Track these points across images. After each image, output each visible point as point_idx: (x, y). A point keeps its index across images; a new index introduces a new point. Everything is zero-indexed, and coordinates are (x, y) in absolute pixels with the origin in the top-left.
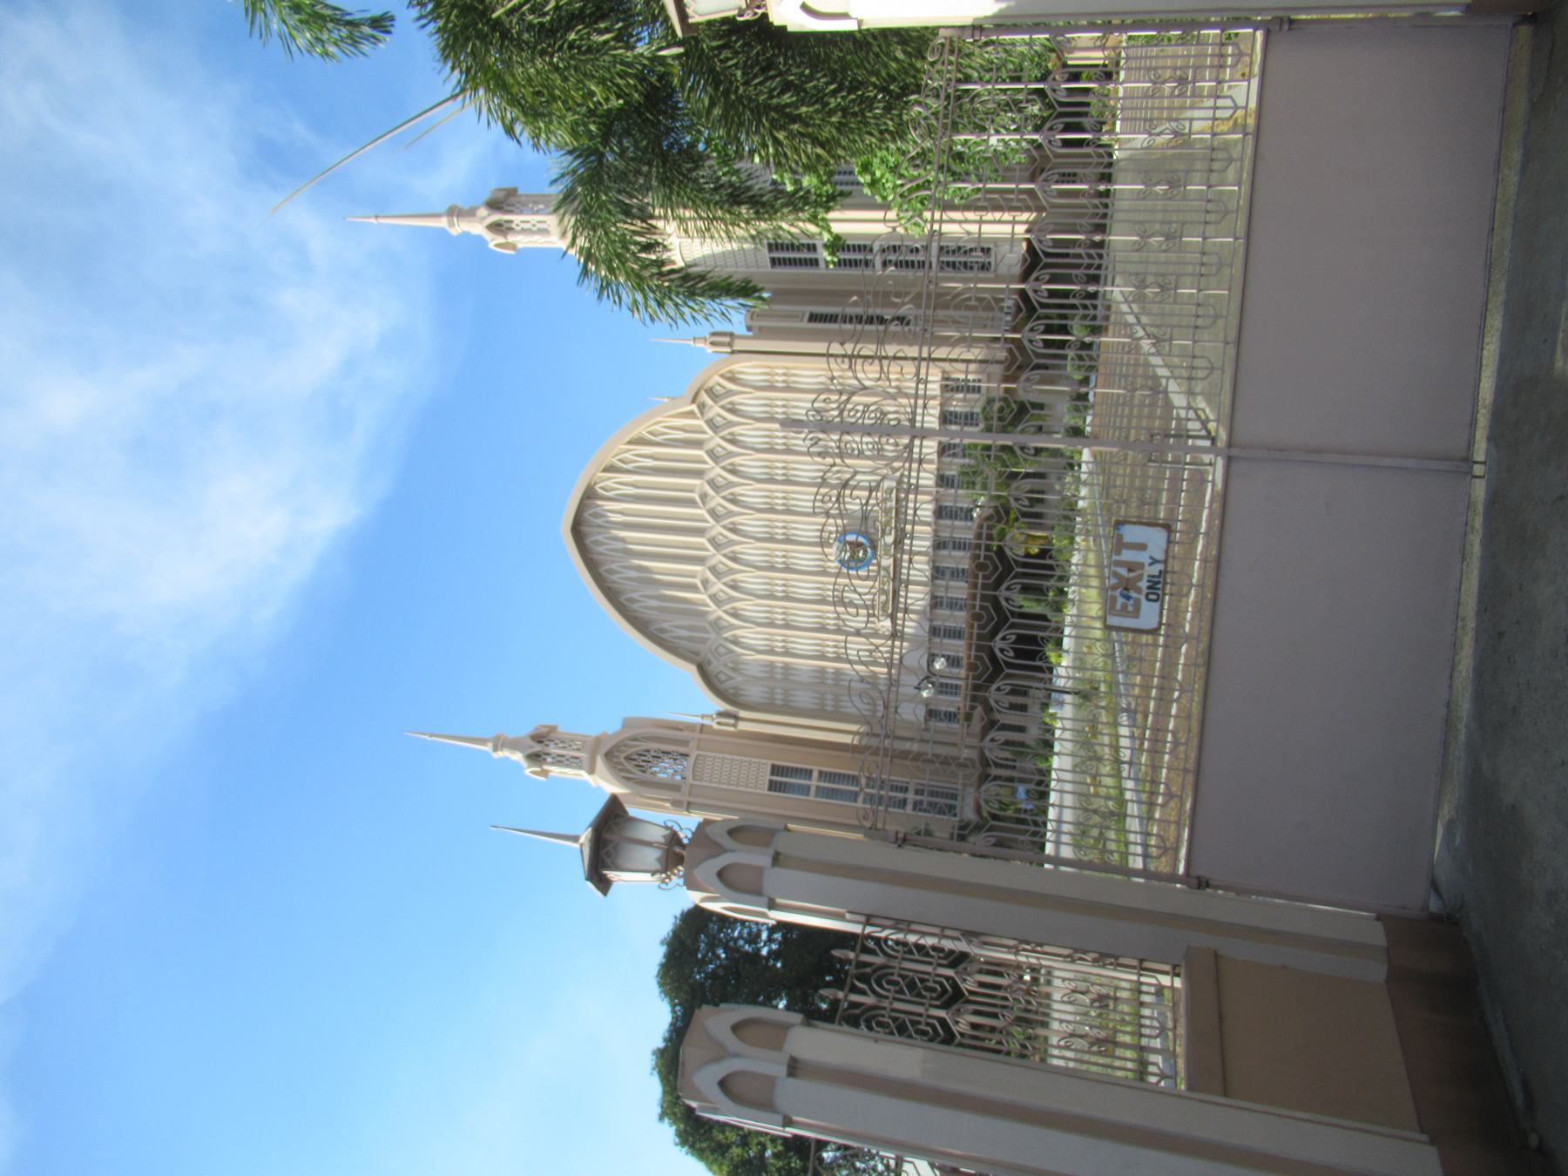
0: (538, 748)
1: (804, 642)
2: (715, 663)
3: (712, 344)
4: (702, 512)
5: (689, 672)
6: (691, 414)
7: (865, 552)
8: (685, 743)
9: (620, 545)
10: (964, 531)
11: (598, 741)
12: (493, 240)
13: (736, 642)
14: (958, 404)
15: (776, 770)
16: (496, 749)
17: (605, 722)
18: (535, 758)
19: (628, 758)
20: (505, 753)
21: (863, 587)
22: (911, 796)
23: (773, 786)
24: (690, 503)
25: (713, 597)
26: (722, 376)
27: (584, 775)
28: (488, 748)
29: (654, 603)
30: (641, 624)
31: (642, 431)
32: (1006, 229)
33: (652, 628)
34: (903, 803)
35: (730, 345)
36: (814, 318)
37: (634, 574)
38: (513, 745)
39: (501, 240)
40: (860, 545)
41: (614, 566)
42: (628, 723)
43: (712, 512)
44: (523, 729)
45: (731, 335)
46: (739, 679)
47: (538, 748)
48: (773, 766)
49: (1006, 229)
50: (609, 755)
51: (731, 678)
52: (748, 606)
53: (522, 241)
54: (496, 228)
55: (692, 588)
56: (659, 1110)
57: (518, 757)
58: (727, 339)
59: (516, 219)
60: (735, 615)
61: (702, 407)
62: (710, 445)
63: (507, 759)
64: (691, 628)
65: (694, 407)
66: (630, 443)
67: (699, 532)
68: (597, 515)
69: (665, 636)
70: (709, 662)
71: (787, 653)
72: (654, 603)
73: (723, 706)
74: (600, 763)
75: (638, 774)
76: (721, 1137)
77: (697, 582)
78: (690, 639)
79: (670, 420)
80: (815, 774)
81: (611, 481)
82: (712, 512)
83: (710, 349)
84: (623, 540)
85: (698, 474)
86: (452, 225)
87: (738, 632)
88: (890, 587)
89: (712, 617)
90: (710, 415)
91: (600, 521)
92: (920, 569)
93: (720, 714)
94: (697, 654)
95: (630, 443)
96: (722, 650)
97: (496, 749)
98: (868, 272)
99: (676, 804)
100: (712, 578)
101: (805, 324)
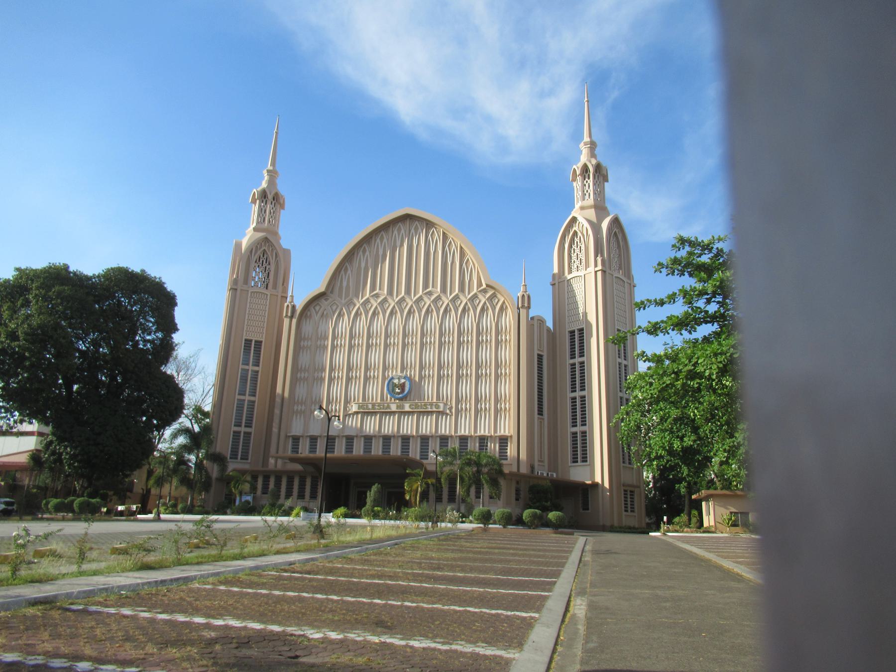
0: (270, 197)
1: (341, 358)
2: (326, 303)
7: (399, 394)
8: (275, 287)
9: (398, 243)
10: (414, 452)
11: (276, 234)
12: (578, 167)
13: (340, 315)
15: (259, 344)
17: (287, 238)
18: (264, 195)
19: (264, 252)
21: (376, 391)
22: (243, 429)
23: (248, 342)
24: (426, 286)
25: (368, 301)
26: (504, 302)
28: (269, 167)
29: (363, 265)
30: (349, 257)
31: (469, 255)
32: (599, 470)
33: (347, 264)
34: (238, 424)
35: (523, 306)
36: (540, 357)
37: (381, 252)
38: (272, 182)
39: (578, 172)
40: (403, 390)
41: (385, 240)
42: (287, 252)
44: (282, 188)
45: (529, 307)
46: (317, 318)
47: (270, 197)
48: (261, 342)
49: (599, 470)
50: (266, 240)
51: (317, 313)
52: (362, 324)
53: (577, 185)
54: (585, 169)
55: (373, 288)
57: (264, 185)
58: (526, 305)
59: (591, 181)
61: (484, 291)
64: (348, 287)
65: (484, 286)
66: (461, 248)
67: (408, 292)
68: (416, 229)
69: (343, 272)
70: (326, 300)
71: (334, 347)
72: (363, 265)
73: (299, 308)
76: (5, 308)
77: (377, 291)
78: (341, 288)
79: (478, 272)
80: (256, 368)
81: (437, 237)
82: (421, 299)
84: (402, 245)
86: (585, 144)
87: (346, 317)
88: (377, 409)
89: (355, 301)
91: (413, 231)
92: (389, 426)
93: (294, 307)
94: (332, 292)
95: (461, 248)
96: (334, 308)
97: (268, 171)
101: (536, 352)
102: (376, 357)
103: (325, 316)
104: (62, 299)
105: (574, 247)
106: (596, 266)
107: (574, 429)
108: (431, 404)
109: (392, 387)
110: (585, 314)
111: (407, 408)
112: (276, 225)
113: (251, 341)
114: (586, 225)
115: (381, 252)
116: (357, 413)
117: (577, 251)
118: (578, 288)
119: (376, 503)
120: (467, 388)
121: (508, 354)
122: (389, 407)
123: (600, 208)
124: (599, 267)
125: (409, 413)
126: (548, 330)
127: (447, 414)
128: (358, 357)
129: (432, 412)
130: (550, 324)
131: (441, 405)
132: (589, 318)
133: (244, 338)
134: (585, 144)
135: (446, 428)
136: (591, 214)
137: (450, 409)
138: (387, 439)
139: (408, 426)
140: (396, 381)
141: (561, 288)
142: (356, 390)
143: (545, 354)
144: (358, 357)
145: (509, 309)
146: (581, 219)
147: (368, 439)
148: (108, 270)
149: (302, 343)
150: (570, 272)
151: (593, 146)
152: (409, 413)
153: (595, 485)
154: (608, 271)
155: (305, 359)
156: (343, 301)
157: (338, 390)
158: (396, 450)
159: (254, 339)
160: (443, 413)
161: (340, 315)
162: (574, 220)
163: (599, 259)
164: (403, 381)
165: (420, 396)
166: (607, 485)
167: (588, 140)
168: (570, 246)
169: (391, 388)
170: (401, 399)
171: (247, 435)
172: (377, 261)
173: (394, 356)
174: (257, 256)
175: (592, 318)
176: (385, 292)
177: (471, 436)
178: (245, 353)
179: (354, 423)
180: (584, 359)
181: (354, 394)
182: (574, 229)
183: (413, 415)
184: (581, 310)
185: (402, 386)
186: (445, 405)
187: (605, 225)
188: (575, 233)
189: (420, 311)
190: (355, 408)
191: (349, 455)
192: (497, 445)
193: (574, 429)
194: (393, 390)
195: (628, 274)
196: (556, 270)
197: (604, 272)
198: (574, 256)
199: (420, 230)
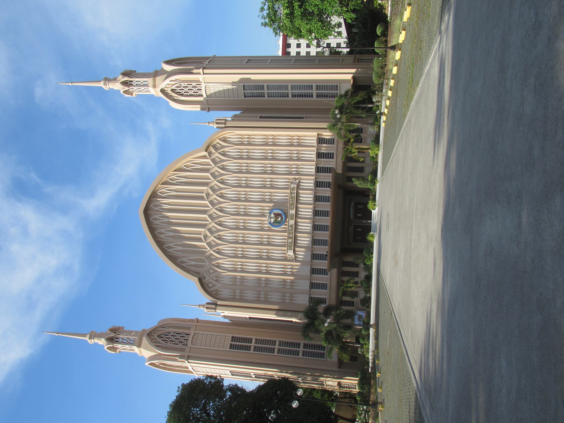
1: (251, 265)
2: (207, 278)
5: (194, 281)
6: (204, 157)
7: (282, 218)
9: (166, 220)
10: (327, 178)
11: (144, 331)
13: (218, 266)
14: (324, 149)
15: (234, 339)
16: (90, 338)
17: (151, 323)
18: (111, 340)
20: (96, 341)
21: (279, 236)
22: (301, 349)
23: (232, 346)
24: (202, 198)
25: (209, 244)
26: (220, 139)
28: (87, 339)
29: (180, 248)
30: (173, 259)
31: (180, 165)
32: (344, 76)
33: (177, 261)
34: (297, 353)
35: (225, 124)
36: (261, 117)
37: (171, 234)
38: (100, 336)
39: (127, 88)
40: (280, 215)
41: (162, 231)
44: (105, 329)
45: (226, 120)
46: (218, 285)
47: (113, 335)
48: (233, 337)
49: (344, 76)
51: (215, 285)
52: (226, 248)
54: (125, 83)
55: (199, 240)
57: (102, 342)
58: (224, 121)
59: (135, 80)
60: (218, 253)
61: (210, 154)
62: (213, 171)
65: (206, 154)
66: (175, 171)
67: (204, 212)
68: (156, 206)
69: (184, 265)
70: (205, 278)
72: (180, 248)
74: (145, 340)
78: (195, 266)
80: (254, 341)
81: (164, 189)
82: (211, 202)
83: (215, 126)
84: (168, 217)
85: (203, 226)
87: (220, 261)
88: (292, 235)
89: (208, 254)
90: (214, 157)
91: (157, 209)
92: (306, 226)
93: (208, 304)
94: (199, 273)
95: (175, 171)
96: (211, 271)
97: (90, 338)
98: (286, 99)
99: (181, 357)
102: (253, 237)
103: (218, 278)
105: (183, 92)
106: (199, 74)
107: (315, 95)
108: (291, 193)
109: (277, 223)
110: (233, 83)
111: (293, 212)
112: (137, 332)
113: (231, 344)
114: (167, 81)
115: (171, 234)
117: (186, 90)
118: (214, 89)
119: (364, 179)
120: (281, 167)
121: (258, 135)
122: (291, 226)
123: (156, 74)
124: (201, 71)
125: (297, 211)
126: (242, 113)
127: (299, 182)
128: (252, 251)
129: (297, 193)
131: (292, 186)
132: (236, 80)
133: (228, 349)
134: (105, 84)
135: (309, 183)
137: (295, 179)
138: (317, 199)
139: (307, 211)
140: (272, 220)
141: (212, 103)
142: (277, 253)
143: (259, 115)
144: (252, 251)
145: (226, 135)
146: (163, 86)
147: (315, 242)
150: (201, 96)
152: (297, 211)
153: (354, 78)
154: (204, 66)
155: (250, 294)
156: (207, 264)
157: (276, 267)
158: (327, 192)
159: (230, 342)
160: (298, 185)
162: (163, 91)
163: (195, 71)
164: (272, 215)
166: (354, 71)
167: (102, 82)
168: (182, 95)
169: (277, 224)
170: (286, 217)
171: (306, 346)
172: (179, 237)
173: (253, 223)
174: (162, 341)
175: (237, 78)
177: (316, 164)
178: (242, 343)
179: (301, 253)
180: (265, 85)
181: (279, 254)
182: (170, 92)
184: (230, 87)
185: (277, 215)
186: (292, 183)
188: (173, 90)
189: (220, 203)
190: (291, 253)
191: (330, 214)
192: (324, 145)
193: (315, 95)
194: (279, 222)
195: (207, 58)
196: (197, 108)
197: (204, 68)
198: (191, 92)
199: (157, 203)
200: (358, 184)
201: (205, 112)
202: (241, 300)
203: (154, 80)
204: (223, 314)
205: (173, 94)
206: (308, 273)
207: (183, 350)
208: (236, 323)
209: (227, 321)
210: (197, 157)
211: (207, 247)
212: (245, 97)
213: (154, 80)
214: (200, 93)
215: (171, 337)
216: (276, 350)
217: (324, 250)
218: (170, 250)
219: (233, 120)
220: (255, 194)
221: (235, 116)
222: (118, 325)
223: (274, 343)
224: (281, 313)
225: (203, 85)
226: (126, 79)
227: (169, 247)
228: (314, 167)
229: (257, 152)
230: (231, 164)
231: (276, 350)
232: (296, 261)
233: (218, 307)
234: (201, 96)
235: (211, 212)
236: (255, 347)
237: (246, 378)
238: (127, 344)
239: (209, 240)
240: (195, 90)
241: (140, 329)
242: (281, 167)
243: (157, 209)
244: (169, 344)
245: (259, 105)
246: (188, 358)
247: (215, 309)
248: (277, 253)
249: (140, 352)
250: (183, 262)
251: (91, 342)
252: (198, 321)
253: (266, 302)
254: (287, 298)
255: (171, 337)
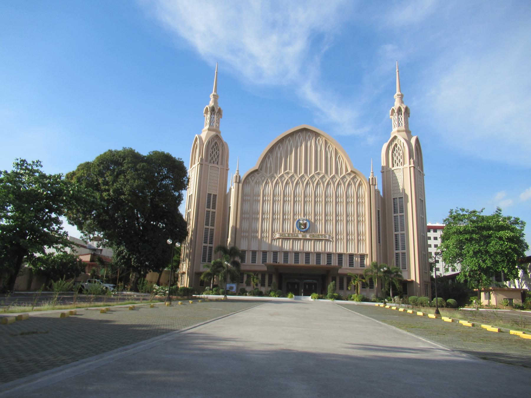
0: (216, 111)
1: (268, 207)
3: (373, 178)
4: (344, 173)
6: (347, 170)
7: (303, 229)
8: (222, 164)
9: (299, 144)
10: (335, 262)
11: (220, 132)
13: (266, 183)
14: (357, 260)
15: (215, 196)
18: (213, 110)
20: (212, 99)
21: (290, 227)
22: (208, 245)
23: (209, 195)
24: (316, 169)
25: (282, 176)
26: (360, 181)
27: (207, 127)
28: (213, 93)
29: (279, 155)
30: (271, 150)
31: (340, 153)
32: (414, 274)
35: (372, 184)
36: (378, 211)
37: (289, 149)
38: (215, 102)
39: (396, 111)
40: (305, 227)
41: (291, 142)
43: (313, 176)
44: (220, 105)
45: (375, 185)
47: (216, 111)
48: (216, 195)
49: (414, 274)
51: (253, 181)
52: (280, 189)
54: (399, 110)
55: (285, 169)
56: (113, 150)
57: (211, 103)
59: (403, 116)
60: (276, 183)
61: (349, 174)
62: (336, 177)
63: (210, 99)
64: (270, 167)
65: (349, 171)
66: (336, 149)
67: (306, 172)
68: (309, 137)
69: (267, 159)
70: (258, 174)
72: (279, 155)
73: (243, 177)
74: (213, 133)
75: (211, 146)
77: (288, 171)
80: (214, 210)
81: (322, 141)
82: (313, 176)
83: (370, 178)
84: (301, 145)
87: (270, 184)
88: (291, 237)
89: (275, 175)
90: (347, 177)
91: (307, 137)
92: (298, 246)
93: (240, 177)
94: (261, 169)
96: (263, 178)
97: (214, 95)
98: (394, 230)
99: (202, 159)
100: (290, 176)
102: (289, 208)
103: (258, 183)
104: (144, 170)
105: (395, 152)
106: (410, 164)
107: (397, 251)
108: (322, 235)
109: (299, 225)
110: (404, 190)
111: (308, 237)
112: (218, 127)
113: (211, 194)
114: (403, 141)
115: (289, 149)
116: (279, 238)
117: (397, 155)
119: (334, 290)
120: (341, 227)
121: (365, 209)
122: (297, 236)
123: (408, 132)
124: (412, 165)
125: (309, 240)
126: (381, 197)
127: (330, 241)
128: (278, 207)
129: (322, 240)
130: (381, 194)
131: (328, 236)
132: (406, 192)
133: (208, 192)
134: (398, 95)
135: (330, 248)
136: (404, 134)
137: (333, 238)
138: (318, 255)
139: (309, 247)
140: (301, 222)
141: (388, 175)
142: (278, 225)
144: (278, 207)
145: (363, 186)
147: (286, 253)
148: (156, 153)
149: (245, 198)
150: (393, 166)
151: (402, 97)
152: (309, 240)
153: (412, 281)
154: (416, 167)
155: (247, 207)
156: (268, 175)
157: (267, 225)
158: (324, 262)
159: (212, 193)
161: (266, 183)
162: (395, 137)
163: (412, 161)
164: (305, 222)
165: (315, 230)
166: (418, 281)
168: (393, 152)
169: (298, 225)
170: (304, 232)
171: (211, 248)
172: (287, 154)
173: (299, 208)
175: (408, 192)
176: (293, 171)
177: (345, 254)
178: (212, 202)
179: (277, 244)
180: (404, 214)
181: (277, 227)
182: (395, 143)
183: (322, 241)
184: (401, 187)
185: (305, 225)
186: (330, 236)
187: (413, 141)
188: (396, 145)
189: (313, 183)
190: (277, 236)
191: (307, 265)
192: (359, 259)
193: (397, 251)
194: (300, 227)
195: (422, 170)
196: (383, 163)
197: (414, 167)
198: (395, 158)
199: (311, 137)
200: (331, 286)
201: (381, 169)
202: (243, 201)
203: (403, 131)
204: (232, 188)
205: (393, 145)
206: (263, 249)
207: (206, 160)
208: (226, 197)
209: (228, 191)
210: (346, 165)
211: (281, 174)
212: (394, 199)
213: (403, 131)
214: (395, 165)
215: (215, 152)
216: (207, 227)
217: (280, 260)
218: (277, 148)
219: (375, 190)
220: (320, 208)
221: (379, 192)
222: (223, 114)
223: (213, 225)
224: (234, 230)
225: (401, 167)
226: (403, 110)
227: (279, 147)
228: (342, 252)
229: (352, 209)
230: (342, 190)
231: (207, 227)
232: (272, 240)
233: (237, 184)
234: (393, 166)
235: (306, 176)
236: (209, 211)
237: (188, 207)
238: (210, 121)
239: (285, 176)
240: (397, 161)
241: (220, 129)
242: (341, 227)
243: (307, 137)
244: (210, 151)
245: (388, 209)
246: (201, 164)
247: (236, 182)
248: (278, 225)
249: (205, 131)
250: (269, 158)
251: (211, 97)
252: (227, 170)
253: (242, 219)
254: (245, 234)
255: (215, 152)
